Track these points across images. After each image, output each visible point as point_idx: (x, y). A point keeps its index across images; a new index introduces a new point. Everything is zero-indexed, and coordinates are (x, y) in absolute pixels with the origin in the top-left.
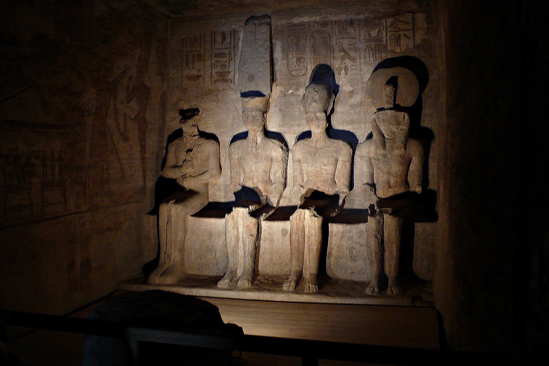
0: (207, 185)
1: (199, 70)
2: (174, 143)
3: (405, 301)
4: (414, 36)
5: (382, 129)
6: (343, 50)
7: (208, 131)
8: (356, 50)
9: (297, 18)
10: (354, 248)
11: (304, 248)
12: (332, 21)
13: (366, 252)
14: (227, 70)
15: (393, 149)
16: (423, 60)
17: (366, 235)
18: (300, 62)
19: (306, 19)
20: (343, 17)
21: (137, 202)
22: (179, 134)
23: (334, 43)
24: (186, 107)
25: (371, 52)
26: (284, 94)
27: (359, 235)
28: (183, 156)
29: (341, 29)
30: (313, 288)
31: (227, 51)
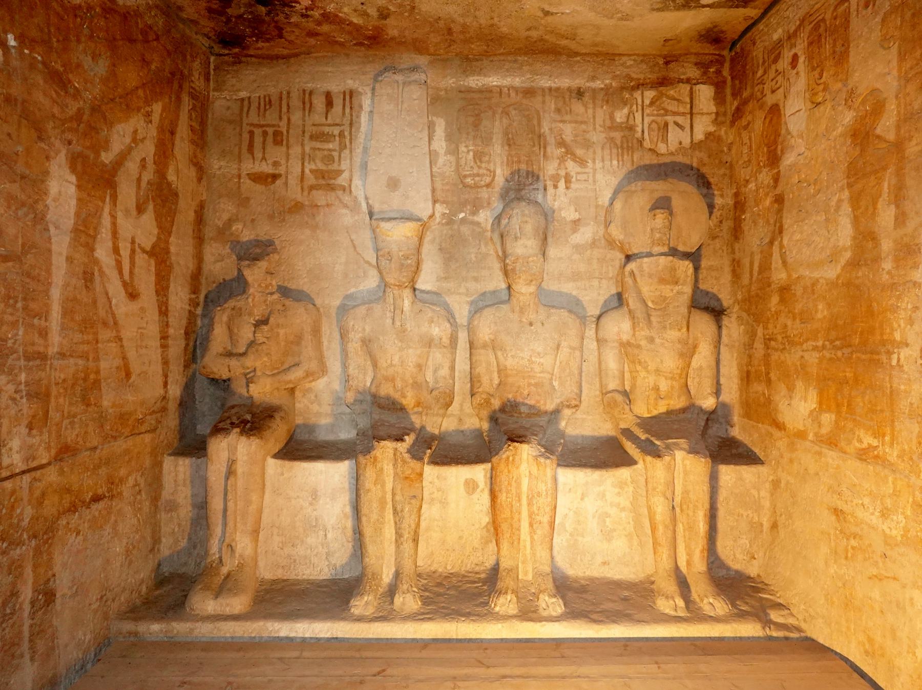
0: (292, 391)
1: (276, 164)
2: (226, 305)
6: (562, 143)
7: (292, 285)
9: (476, 78)
10: (608, 515)
11: (519, 520)
12: (543, 89)
14: (335, 167)
15: (665, 328)
17: (631, 489)
18: (481, 161)
19: (494, 80)
20: (565, 82)
21: (153, 430)
23: (545, 129)
24: (247, 236)
25: (614, 151)
26: (449, 221)
27: (617, 490)
28: (246, 333)
29: (560, 104)
30: (555, 606)
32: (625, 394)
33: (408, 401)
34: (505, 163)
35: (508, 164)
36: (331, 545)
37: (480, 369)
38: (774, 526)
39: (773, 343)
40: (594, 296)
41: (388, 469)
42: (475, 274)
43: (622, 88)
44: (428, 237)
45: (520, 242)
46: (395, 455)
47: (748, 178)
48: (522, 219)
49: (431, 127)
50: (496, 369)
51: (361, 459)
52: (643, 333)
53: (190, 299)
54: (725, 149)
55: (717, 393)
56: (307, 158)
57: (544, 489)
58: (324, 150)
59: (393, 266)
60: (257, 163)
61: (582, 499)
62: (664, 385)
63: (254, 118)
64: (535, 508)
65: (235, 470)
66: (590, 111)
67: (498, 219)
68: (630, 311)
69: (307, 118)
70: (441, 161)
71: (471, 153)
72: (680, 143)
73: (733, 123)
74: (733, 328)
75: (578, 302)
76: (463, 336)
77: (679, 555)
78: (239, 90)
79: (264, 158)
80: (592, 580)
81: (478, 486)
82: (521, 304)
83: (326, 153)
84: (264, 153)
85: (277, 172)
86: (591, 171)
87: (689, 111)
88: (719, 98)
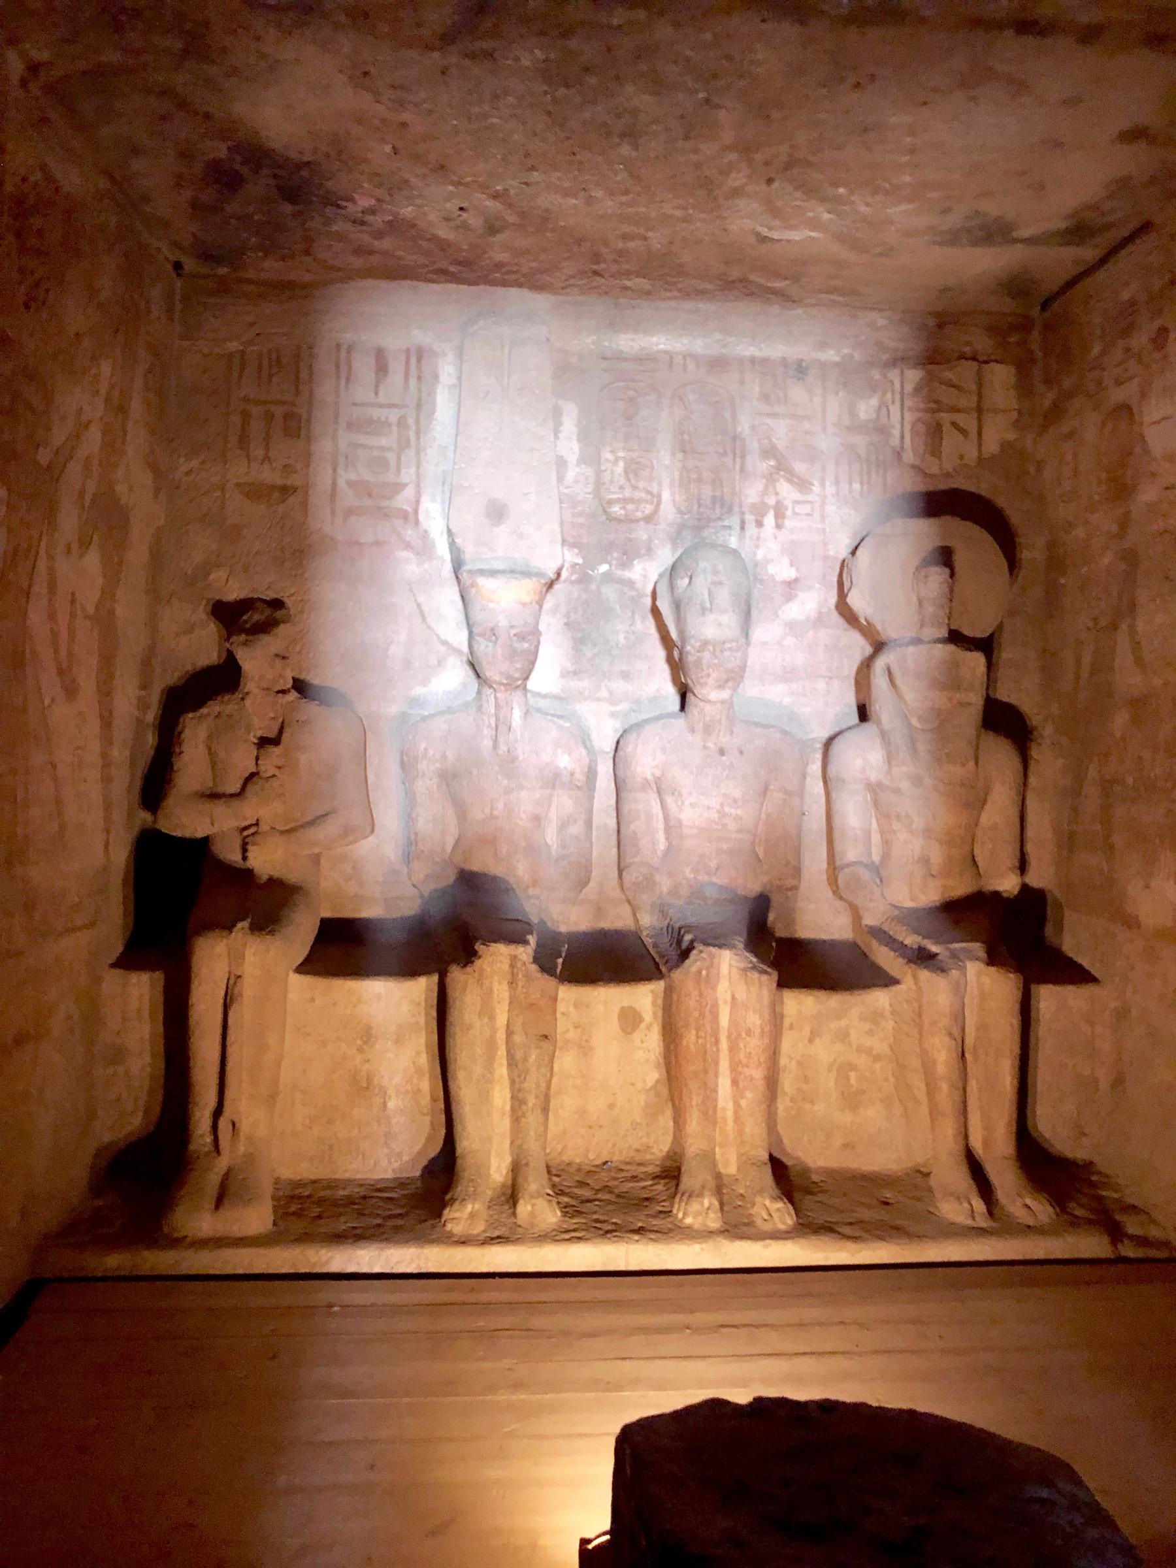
0: (316, 859)
1: (287, 468)
2: (204, 711)
3: (1091, 1245)
4: (980, 433)
5: (910, 696)
6: (769, 452)
7: (314, 678)
8: (812, 456)
10: (852, 1067)
11: (716, 1075)
12: (740, 361)
13: (892, 1079)
14: (390, 477)
16: (1001, 502)
17: (890, 1024)
19: (660, 342)
20: (776, 350)
22: (222, 679)
23: (744, 426)
24: (234, 593)
26: (583, 579)
27: (867, 1026)
31: (393, 416)
34: (677, 483)
35: (681, 485)
36: (394, 1121)
37: (635, 826)
38: (1118, 1082)
39: (1117, 788)
41: (501, 991)
42: (625, 668)
43: (870, 364)
44: (547, 605)
45: (710, 617)
46: (512, 966)
47: (1071, 518)
49: (557, 414)
50: (661, 825)
51: (456, 974)
52: (905, 769)
53: (139, 698)
54: (1032, 470)
55: (1023, 866)
56: (342, 460)
57: (758, 1022)
58: (371, 448)
59: (499, 651)
60: (254, 465)
61: (811, 1041)
64: (742, 1056)
65: (241, 995)
66: (818, 400)
68: (884, 735)
69: (342, 393)
70: (571, 473)
71: (621, 464)
72: (961, 457)
73: (1045, 428)
74: (1048, 761)
77: (971, 1130)
78: (225, 340)
79: (267, 458)
80: (831, 1173)
81: (641, 1020)
82: (707, 718)
83: (375, 453)
84: (267, 448)
85: (289, 482)
86: (817, 499)
87: (974, 405)
88: (1024, 387)
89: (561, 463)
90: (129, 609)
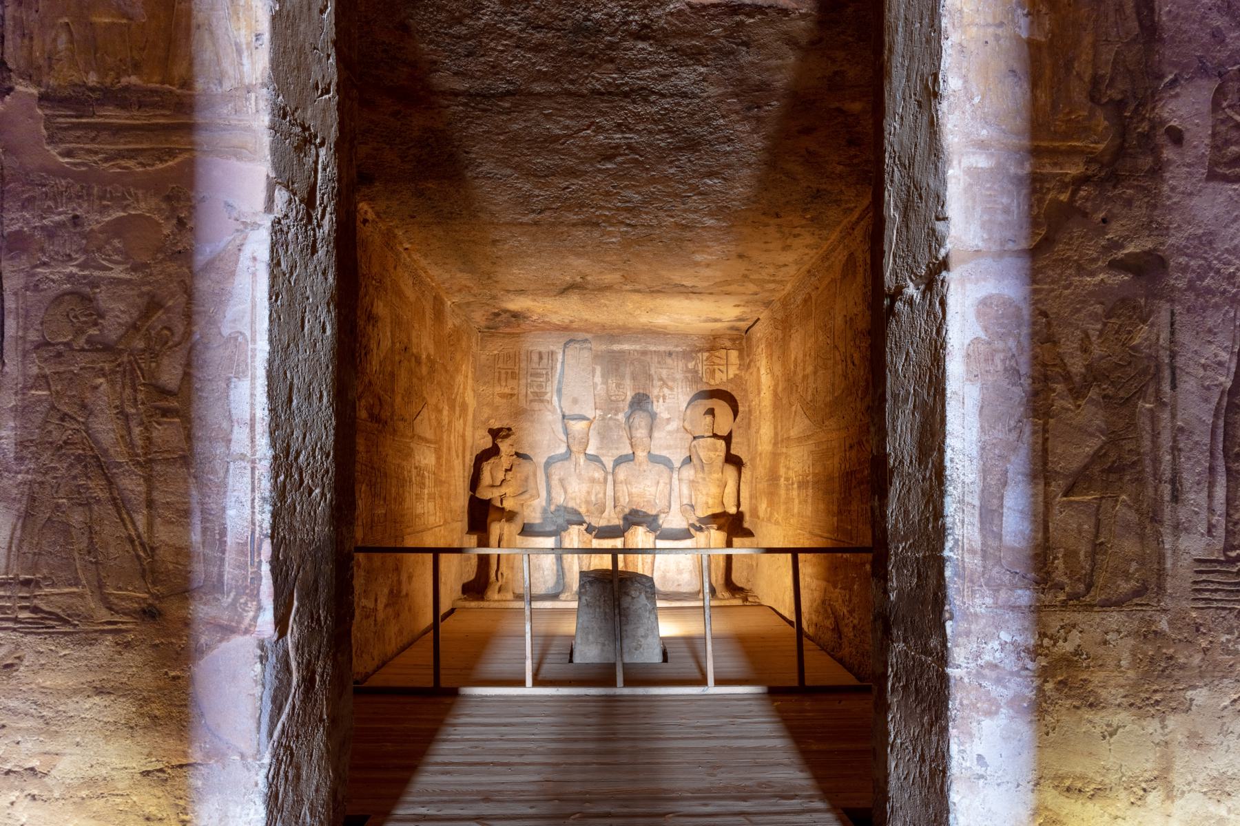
5: (702, 455)
6: (661, 379)
7: (521, 451)
8: (674, 380)
19: (626, 347)
20: (662, 348)
22: (493, 452)
23: (652, 372)
24: (496, 426)
26: (603, 419)
32: (692, 506)
33: (583, 510)
37: (619, 494)
40: (677, 458)
48: (640, 420)
49: (594, 371)
55: (738, 505)
62: (711, 502)
63: (501, 365)
67: (628, 418)
74: (746, 473)
75: (669, 460)
76: (610, 478)
88: (741, 357)
89: (595, 386)
90: (468, 433)
